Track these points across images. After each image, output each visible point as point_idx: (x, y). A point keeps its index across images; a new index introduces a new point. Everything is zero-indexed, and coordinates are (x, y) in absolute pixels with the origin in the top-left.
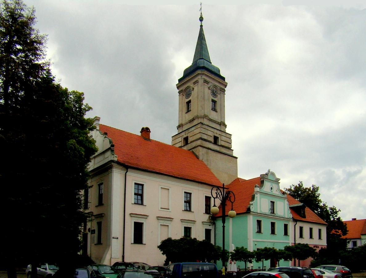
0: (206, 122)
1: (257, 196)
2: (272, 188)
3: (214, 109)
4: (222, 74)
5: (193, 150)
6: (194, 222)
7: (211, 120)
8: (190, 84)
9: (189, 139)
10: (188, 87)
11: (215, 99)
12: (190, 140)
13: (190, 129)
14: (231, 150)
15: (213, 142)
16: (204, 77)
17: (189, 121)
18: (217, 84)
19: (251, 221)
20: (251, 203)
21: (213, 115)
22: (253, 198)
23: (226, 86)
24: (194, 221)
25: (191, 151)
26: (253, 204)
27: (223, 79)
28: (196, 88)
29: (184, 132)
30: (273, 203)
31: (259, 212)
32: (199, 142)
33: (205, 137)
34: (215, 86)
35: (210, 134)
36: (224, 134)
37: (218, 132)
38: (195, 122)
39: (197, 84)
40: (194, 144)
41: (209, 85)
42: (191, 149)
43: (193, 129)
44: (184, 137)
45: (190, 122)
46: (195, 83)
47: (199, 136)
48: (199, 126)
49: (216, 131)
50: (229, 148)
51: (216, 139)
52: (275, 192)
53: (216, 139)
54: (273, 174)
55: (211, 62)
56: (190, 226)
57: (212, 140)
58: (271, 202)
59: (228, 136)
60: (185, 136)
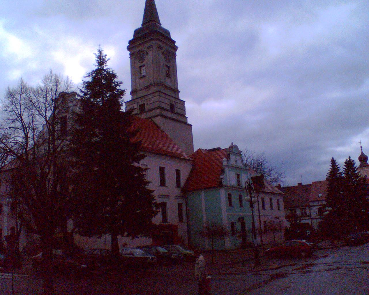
0: (162, 89)
1: (227, 170)
2: (236, 161)
3: (168, 75)
4: (173, 37)
5: (153, 119)
6: (168, 196)
7: (166, 87)
8: (144, 48)
9: (146, 106)
10: (142, 51)
11: (169, 65)
12: (147, 107)
13: (147, 96)
14: (186, 117)
15: (169, 109)
16: (158, 42)
17: (144, 87)
18: (170, 49)
19: (223, 194)
20: (221, 177)
21: (168, 82)
22: (223, 171)
23: (176, 50)
24: (168, 196)
25: (150, 120)
26: (223, 178)
27: (174, 42)
28: (150, 54)
29: (140, 99)
30: (238, 175)
31: (229, 185)
32: (158, 111)
33: (163, 105)
34: (168, 51)
35: (166, 103)
36: (178, 101)
37: (174, 100)
38: (152, 90)
39: (151, 49)
40: (153, 113)
41: (162, 51)
42: (150, 118)
43: (150, 97)
44: (140, 104)
45: (145, 89)
46: (148, 48)
47: (157, 104)
48: (157, 94)
49: (171, 99)
50: (183, 115)
51: (172, 106)
52: (239, 164)
53: (172, 106)
54: (236, 147)
55: (161, 23)
56: (165, 202)
57: (168, 107)
58: (237, 174)
59: (182, 102)
60: (142, 103)
